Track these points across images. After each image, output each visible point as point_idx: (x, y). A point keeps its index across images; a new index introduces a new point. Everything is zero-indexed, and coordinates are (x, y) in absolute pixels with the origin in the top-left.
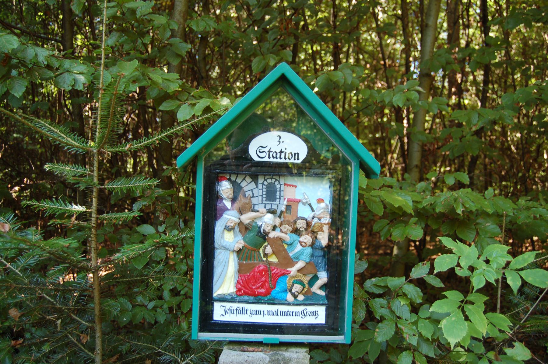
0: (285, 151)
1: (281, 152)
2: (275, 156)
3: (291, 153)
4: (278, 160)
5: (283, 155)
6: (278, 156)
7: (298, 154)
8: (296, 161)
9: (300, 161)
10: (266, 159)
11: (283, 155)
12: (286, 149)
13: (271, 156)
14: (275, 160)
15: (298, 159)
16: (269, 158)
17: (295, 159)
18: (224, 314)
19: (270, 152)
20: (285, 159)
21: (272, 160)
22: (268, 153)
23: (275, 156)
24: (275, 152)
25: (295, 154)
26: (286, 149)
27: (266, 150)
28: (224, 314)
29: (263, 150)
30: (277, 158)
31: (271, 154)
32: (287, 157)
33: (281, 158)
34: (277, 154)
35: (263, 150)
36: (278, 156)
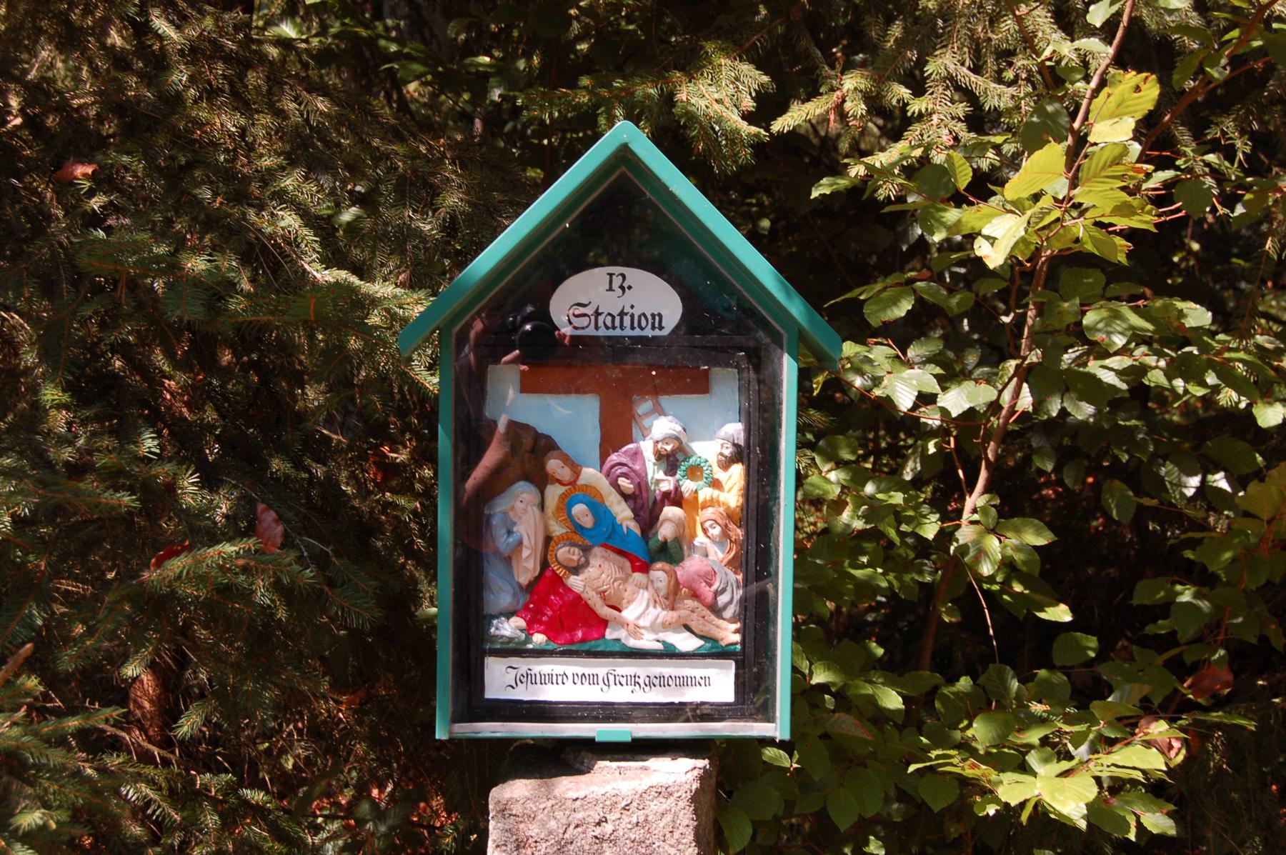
0: (631, 311)
1: (622, 314)
2: (609, 323)
3: (644, 315)
4: (618, 332)
5: (627, 320)
6: (617, 323)
7: (660, 315)
8: (657, 333)
9: (665, 332)
10: (591, 331)
11: (627, 320)
12: (632, 307)
13: (600, 323)
14: (611, 333)
15: (661, 328)
16: (597, 328)
17: (653, 328)
18: (514, 685)
19: (597, 314)
20: (633, 328)
21: (602, 332)
22: (593, 318)
23: (609, 323)
24: (609, 314)
25: (653, 316)
26: (632, 307)
27: (589, 311)
28: (514, 685)
29: (581, 310)
30: (614, 328)
31: (601, 319)
32: (636, 325)
33: (622, 327)
34: (613, 317)
35: (581, 310)
36: (617, 323)
